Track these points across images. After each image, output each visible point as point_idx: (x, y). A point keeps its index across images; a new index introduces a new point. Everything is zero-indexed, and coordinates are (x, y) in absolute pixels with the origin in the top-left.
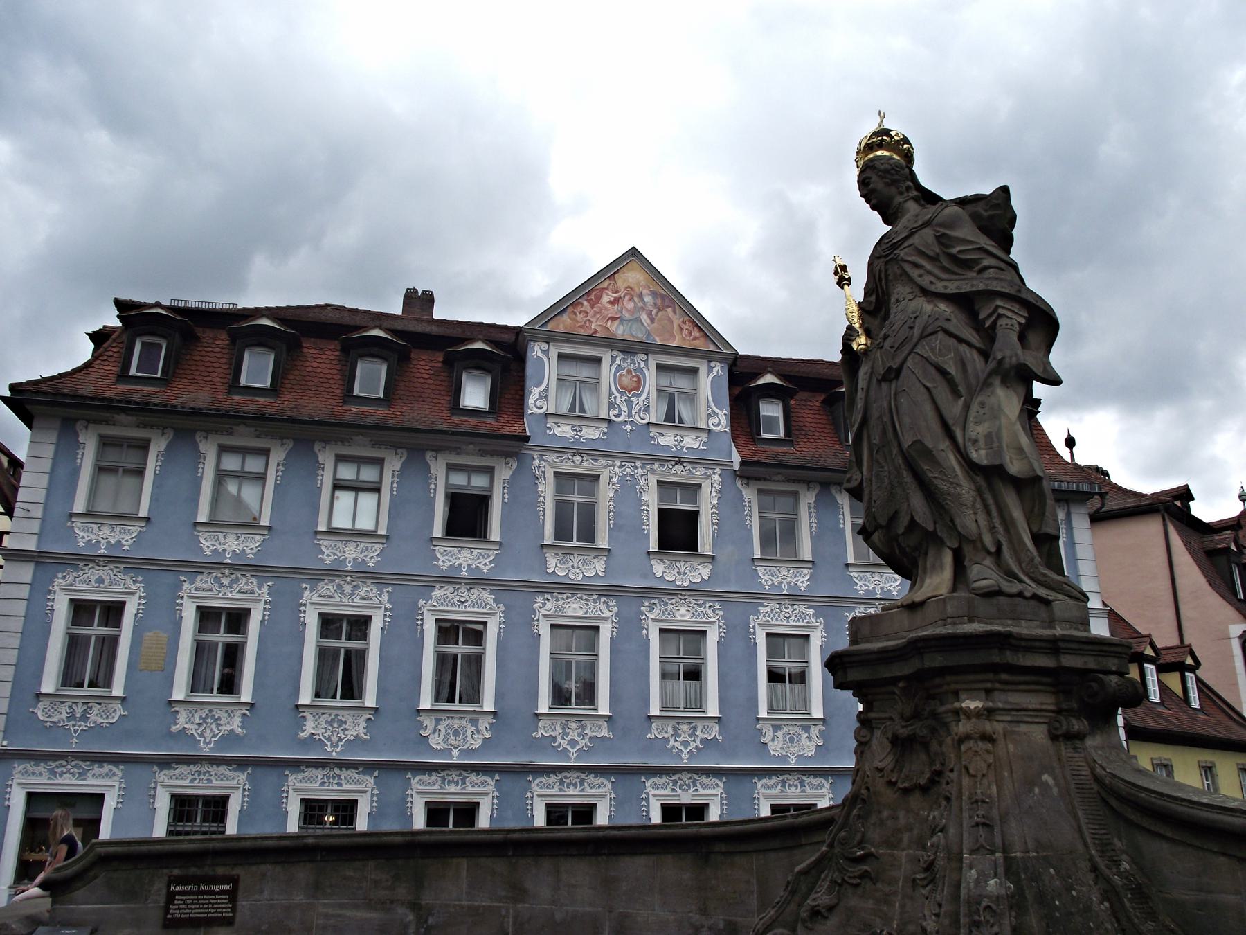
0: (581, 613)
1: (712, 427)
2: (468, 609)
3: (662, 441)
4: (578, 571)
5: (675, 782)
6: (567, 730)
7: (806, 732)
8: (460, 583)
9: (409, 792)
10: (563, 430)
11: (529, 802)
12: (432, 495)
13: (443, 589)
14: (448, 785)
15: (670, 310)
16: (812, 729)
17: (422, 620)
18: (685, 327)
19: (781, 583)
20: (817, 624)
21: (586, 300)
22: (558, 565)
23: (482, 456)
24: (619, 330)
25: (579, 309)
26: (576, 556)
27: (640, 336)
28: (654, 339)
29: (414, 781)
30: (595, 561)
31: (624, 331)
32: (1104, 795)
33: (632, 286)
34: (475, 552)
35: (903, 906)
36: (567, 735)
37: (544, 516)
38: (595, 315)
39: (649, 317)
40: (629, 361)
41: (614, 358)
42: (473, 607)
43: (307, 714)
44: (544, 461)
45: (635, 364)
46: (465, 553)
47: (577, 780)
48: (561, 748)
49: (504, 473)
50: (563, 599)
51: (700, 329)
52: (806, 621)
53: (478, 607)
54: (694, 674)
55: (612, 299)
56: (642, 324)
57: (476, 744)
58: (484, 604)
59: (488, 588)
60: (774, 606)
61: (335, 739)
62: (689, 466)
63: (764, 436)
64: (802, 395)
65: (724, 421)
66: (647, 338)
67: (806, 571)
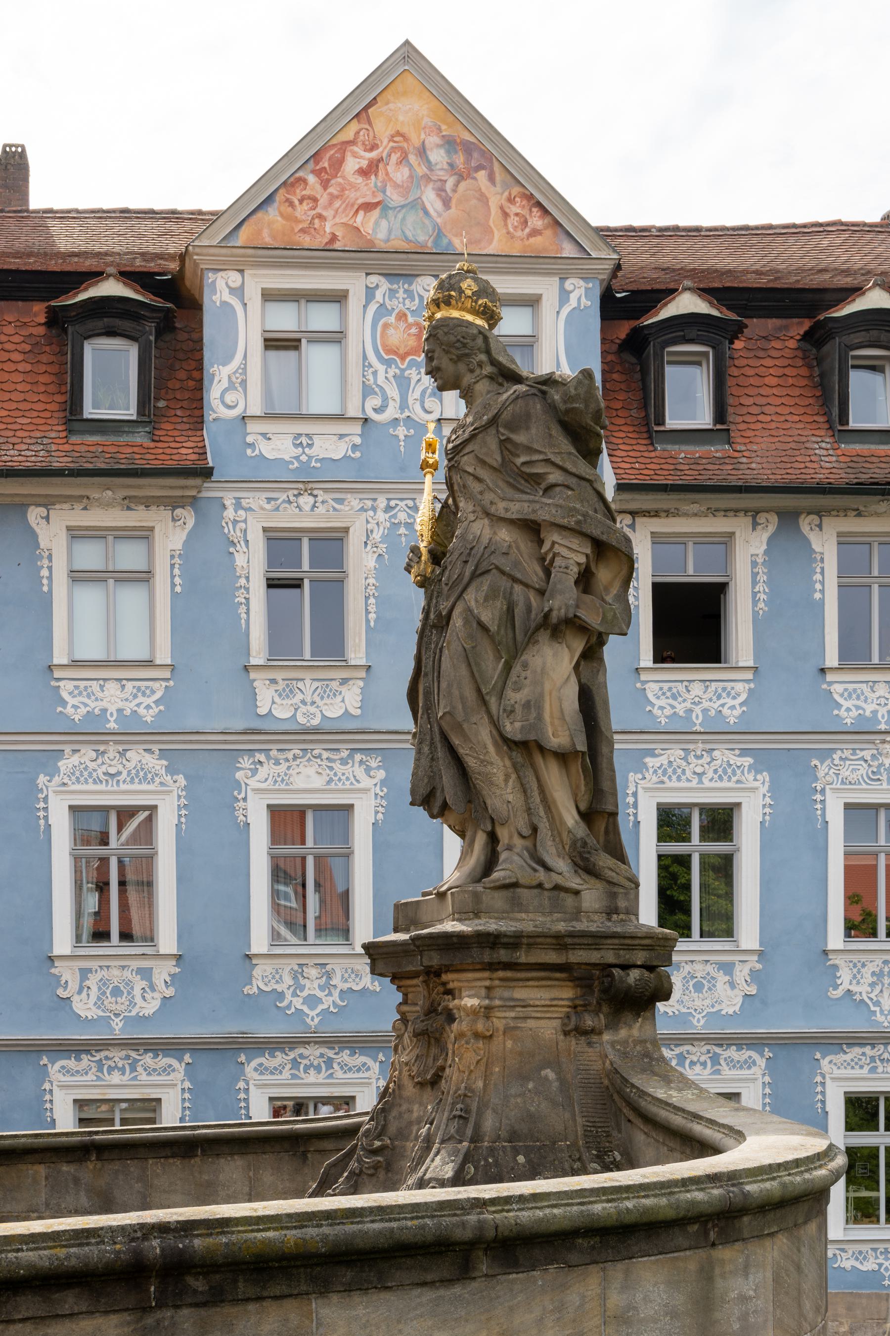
0: (318, 782)
2: (123, 787)
4: (312, 709)
6: (303, 982)
7: (725, 974)
8: (106, 742)
9: (47, 1086)
11: (242, 1096)
12: (45, 589)
13: (77, 755)
14: (109, 1074)
16: (738, 967)
17: (46, 809)
19: (690, 711)
20: (756, 784)
21: (313, 172)
22: (277, 699)
23: (129, 508)
25: (299, 192)
26: (308, 682)
28: (450, 243)
29: (54, 1069)
30: (344, 689)
31: (390, 231)
33: (404, 130)
34: (129, 685)
36: (302, 989)
37: (248, 613)
38: (330, 204)
39: (438, 195)
40: (401, 294)
41: (370, 292)
42: (132, 781)
44: (246, 510)
45: (413, 300)
46: (112, 688)
47: (321, 1060)
48: (293, 1010)
50: (287, 760)
52: (734, 779)
53: (140, 783)
55: (364, 164)
56: (426, 213)
57: (151, 1007)
58: (150, 776)
59: (155, 748)
60: (676, 753)
63: (671, 423)
64: (756, 326)
66: (436, 242)
67: (739, 687)
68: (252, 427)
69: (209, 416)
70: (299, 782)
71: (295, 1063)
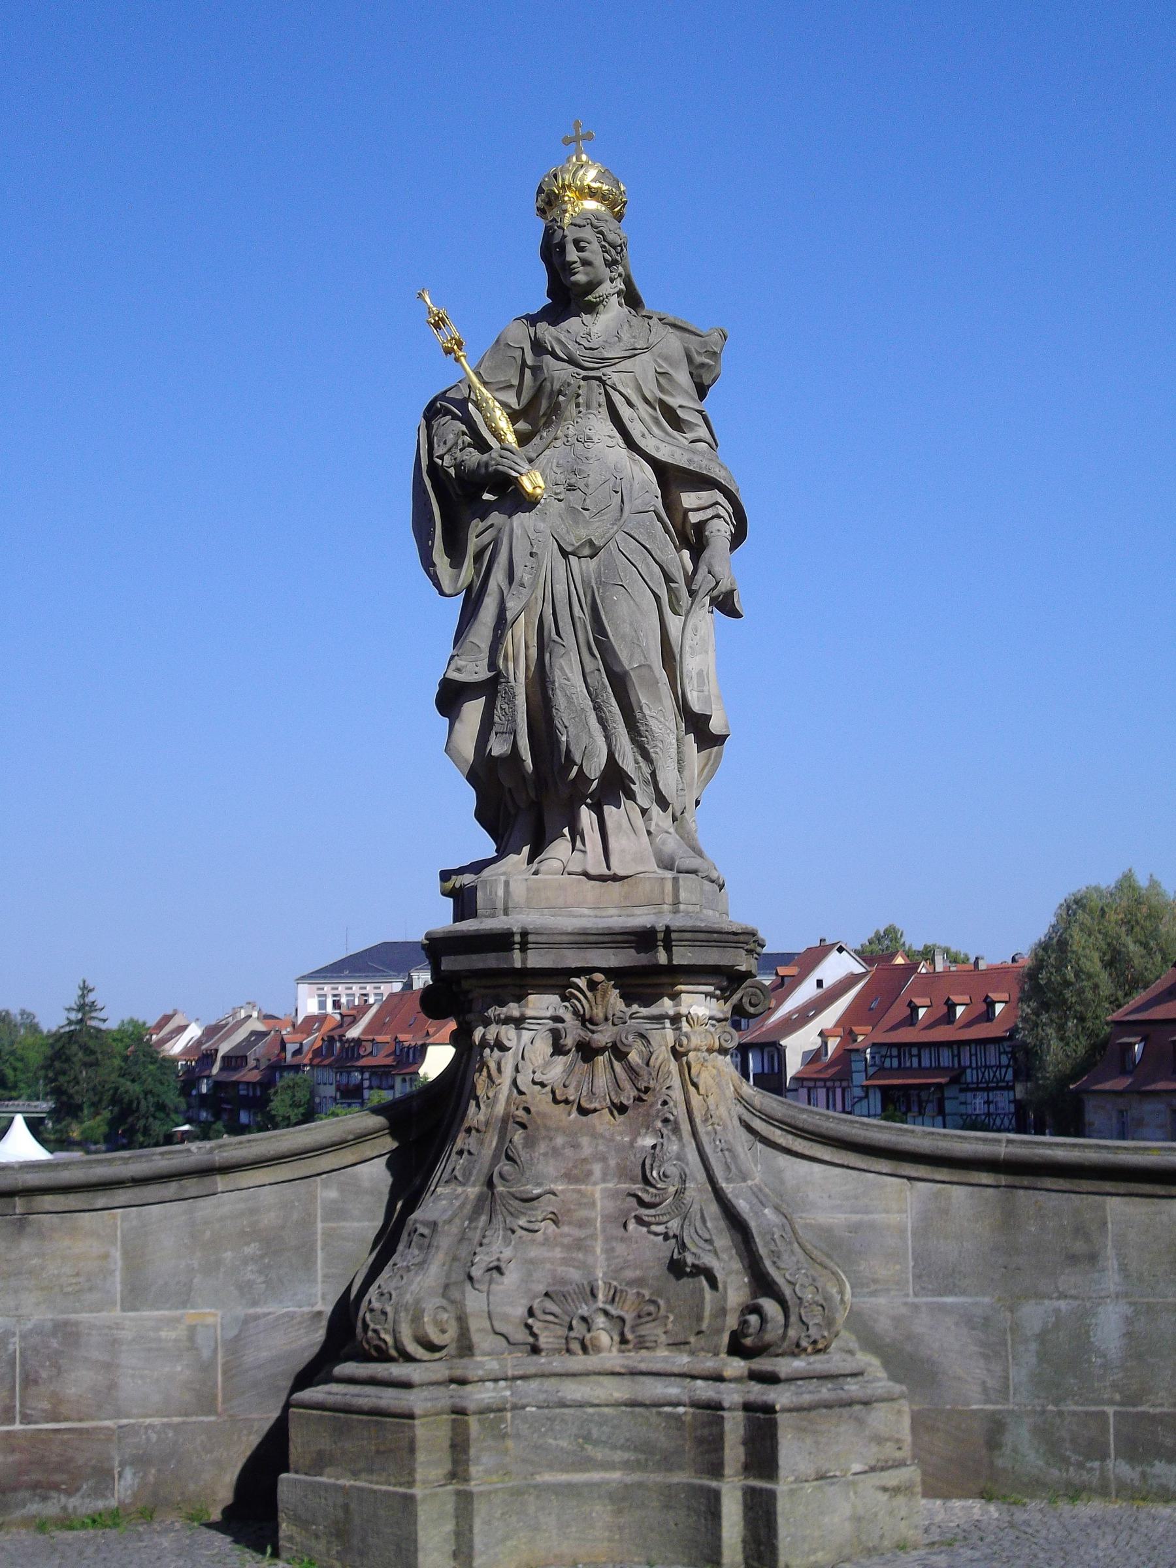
32: (747, 1116)
35: (609, 1251)
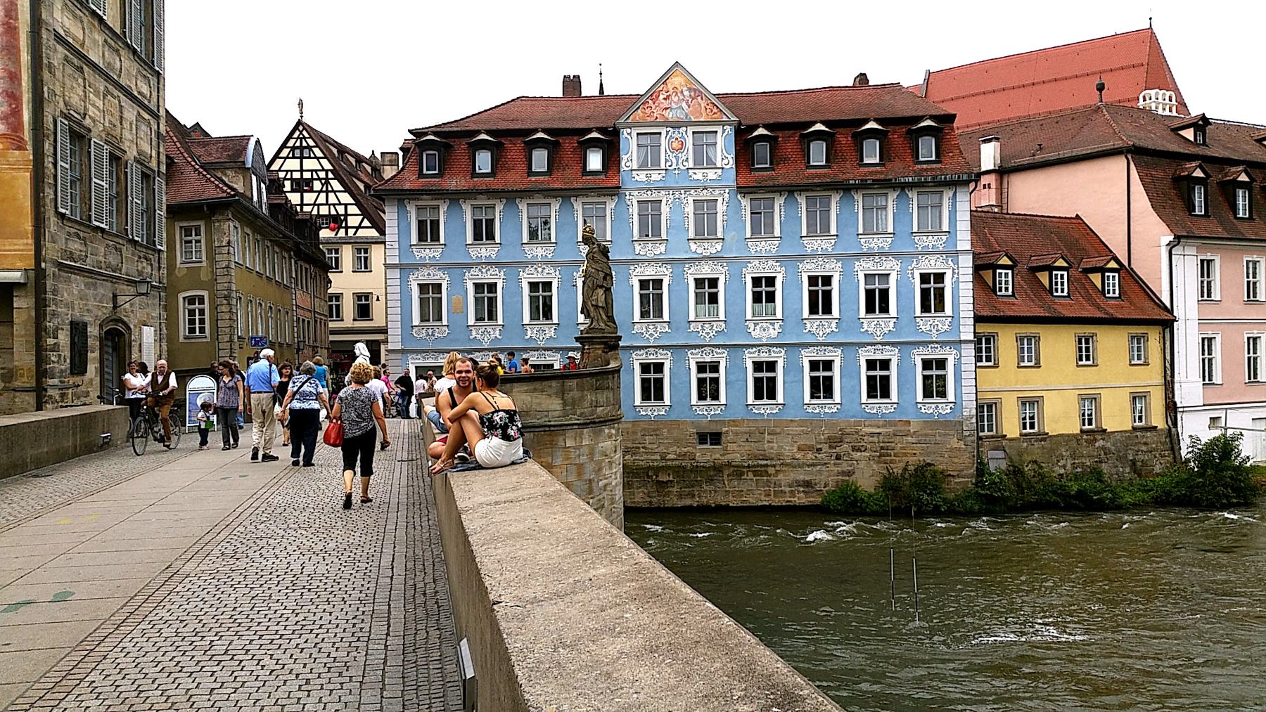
0: (653, 273)
1: (724, 166)
3: (695, 177)
5: (702, 352)
10: (641, 177)
15: (699, 98)
18: (708, 107)
24: (670, 115)
27: (681, 116)
43: (528, 327)
49: (611, 205)
51: (718, 107)
54: (713, 299)
60: (756, 262)
61: (541, 338)
62: (711, 190)
65: (731, 162)
68: (634, 172)
69: (622, 170)
70: (647, 273)
71: (647, 353)
